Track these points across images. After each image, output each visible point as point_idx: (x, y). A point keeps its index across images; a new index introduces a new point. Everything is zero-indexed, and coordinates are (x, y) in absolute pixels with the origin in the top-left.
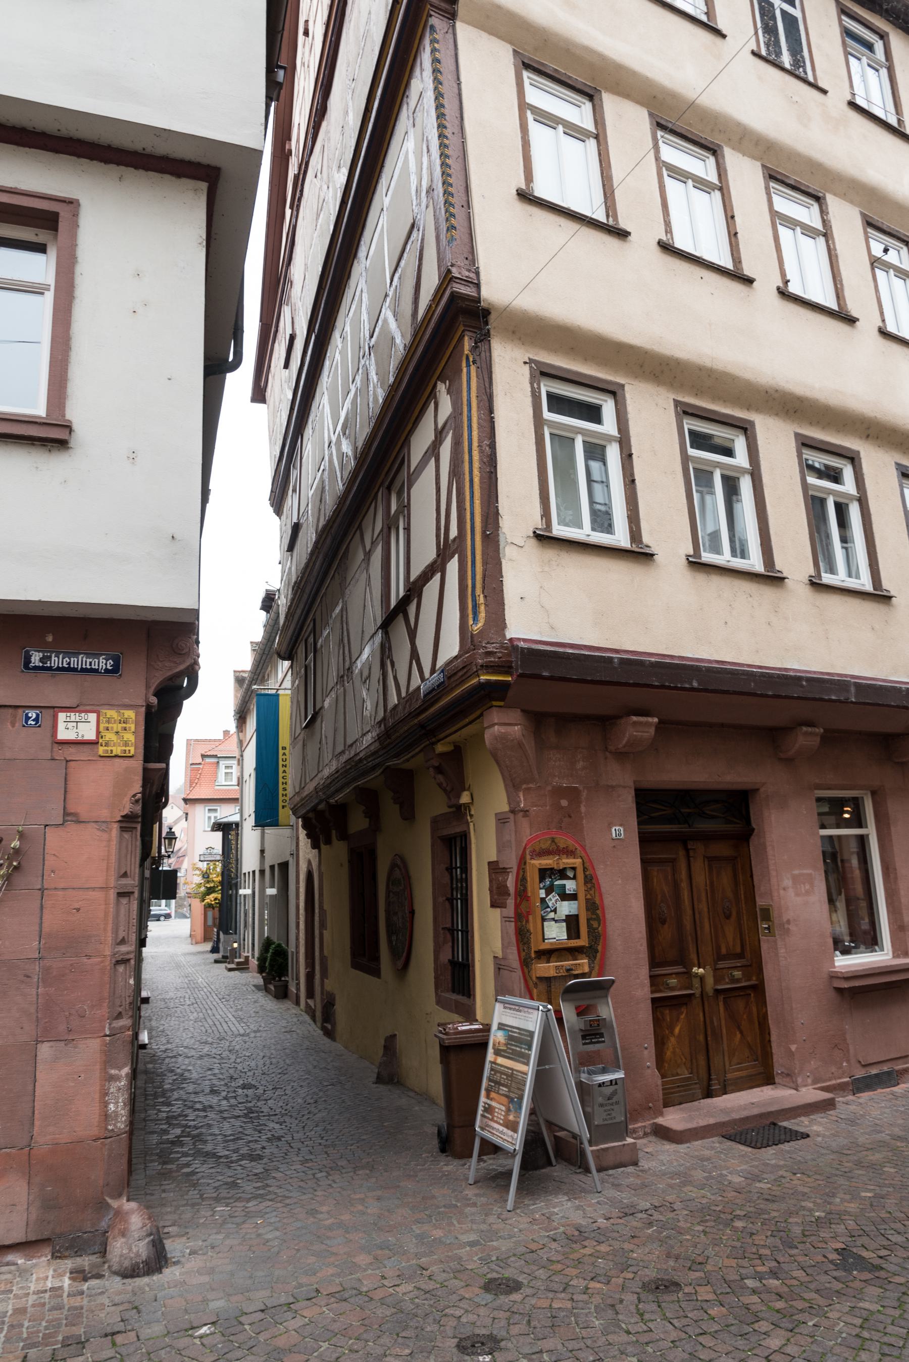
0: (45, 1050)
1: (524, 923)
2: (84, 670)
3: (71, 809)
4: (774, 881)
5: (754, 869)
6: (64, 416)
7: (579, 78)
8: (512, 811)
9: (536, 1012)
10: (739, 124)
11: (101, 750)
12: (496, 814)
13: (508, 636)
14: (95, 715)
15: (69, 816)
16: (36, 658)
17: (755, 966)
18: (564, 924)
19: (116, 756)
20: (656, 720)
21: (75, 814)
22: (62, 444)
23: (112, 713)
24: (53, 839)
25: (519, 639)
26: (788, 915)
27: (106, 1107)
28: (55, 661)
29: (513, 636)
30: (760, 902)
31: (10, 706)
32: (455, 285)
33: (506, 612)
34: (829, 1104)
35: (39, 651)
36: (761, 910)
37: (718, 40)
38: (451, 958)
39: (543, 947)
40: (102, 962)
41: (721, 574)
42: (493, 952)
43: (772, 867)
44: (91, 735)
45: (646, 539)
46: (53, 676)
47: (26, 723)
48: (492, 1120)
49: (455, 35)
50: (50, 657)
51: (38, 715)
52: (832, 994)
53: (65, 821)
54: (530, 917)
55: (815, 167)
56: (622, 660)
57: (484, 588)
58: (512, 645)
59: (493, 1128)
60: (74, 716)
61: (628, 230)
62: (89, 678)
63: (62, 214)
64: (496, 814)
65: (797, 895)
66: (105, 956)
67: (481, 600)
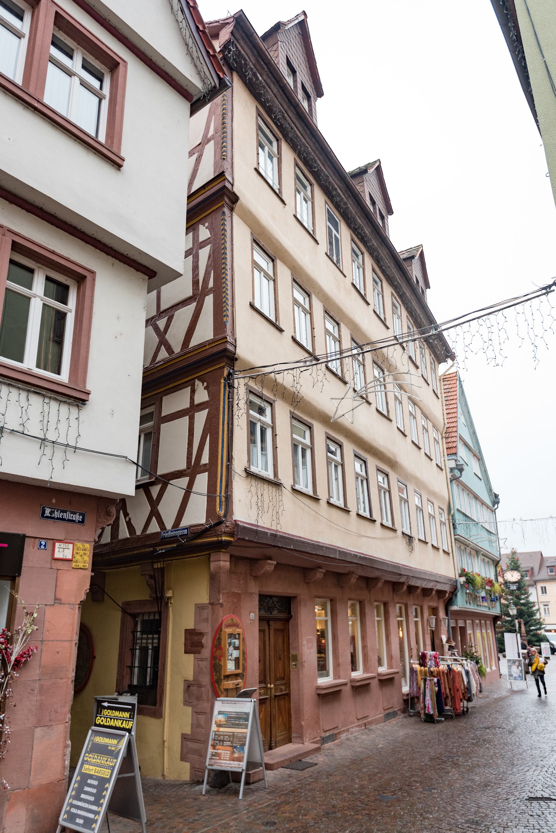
0: (38, 732)
1: (218, 661)
2: (69, 520)
3: (58, 596)
4: (300, 641)
5: (290, 635)
6: (85, 387)
7: (270, 252)
8: (211, 604)
9: (250, 703)
10: (320, 286)
11: (74, 565)
12: (196, 604)
13: (234, 519)
14: (72, 545)
15: (57, 601)
16: (47, 512)
17: (288, 685)
18: (234, 662)
19: (80, 568)
20: (275, 563)
21: (59, 599)
23: (79, 545)
24: (49, 612)
25: (241, 521)
26: (305, 658)
27: (64, 762)
28: (57, 514)
29: (237, 519)
30: (292, 652)
31: (33, 537)
32: (228, 345)
33: (234, 507)
34: (318, 750)
35: (49, 508)
36: (292, 655)
37: (316, 245)
38: (129, 683)
39: (227, 673)
40: (67, 681)
41: (301, 495)
42: (184, 678)
43: (300, 635)
44: (69, 557)
46: (54, 522)
47: (40, 547)
48: (220, 759)
49: (232, 219)
50: (54, 512)
51: (46, 543)
52: (316, 696)
53: (55, 603)
54: (222, 659)
55: (340, 311)
58: (236, 524)
59: (221, 763)
60: (63, 545)
61: (283, 329)
62: (70, 524)
63: (88, 278)
64: (196, 604)
65: (308, 648)
66: (69, 678)
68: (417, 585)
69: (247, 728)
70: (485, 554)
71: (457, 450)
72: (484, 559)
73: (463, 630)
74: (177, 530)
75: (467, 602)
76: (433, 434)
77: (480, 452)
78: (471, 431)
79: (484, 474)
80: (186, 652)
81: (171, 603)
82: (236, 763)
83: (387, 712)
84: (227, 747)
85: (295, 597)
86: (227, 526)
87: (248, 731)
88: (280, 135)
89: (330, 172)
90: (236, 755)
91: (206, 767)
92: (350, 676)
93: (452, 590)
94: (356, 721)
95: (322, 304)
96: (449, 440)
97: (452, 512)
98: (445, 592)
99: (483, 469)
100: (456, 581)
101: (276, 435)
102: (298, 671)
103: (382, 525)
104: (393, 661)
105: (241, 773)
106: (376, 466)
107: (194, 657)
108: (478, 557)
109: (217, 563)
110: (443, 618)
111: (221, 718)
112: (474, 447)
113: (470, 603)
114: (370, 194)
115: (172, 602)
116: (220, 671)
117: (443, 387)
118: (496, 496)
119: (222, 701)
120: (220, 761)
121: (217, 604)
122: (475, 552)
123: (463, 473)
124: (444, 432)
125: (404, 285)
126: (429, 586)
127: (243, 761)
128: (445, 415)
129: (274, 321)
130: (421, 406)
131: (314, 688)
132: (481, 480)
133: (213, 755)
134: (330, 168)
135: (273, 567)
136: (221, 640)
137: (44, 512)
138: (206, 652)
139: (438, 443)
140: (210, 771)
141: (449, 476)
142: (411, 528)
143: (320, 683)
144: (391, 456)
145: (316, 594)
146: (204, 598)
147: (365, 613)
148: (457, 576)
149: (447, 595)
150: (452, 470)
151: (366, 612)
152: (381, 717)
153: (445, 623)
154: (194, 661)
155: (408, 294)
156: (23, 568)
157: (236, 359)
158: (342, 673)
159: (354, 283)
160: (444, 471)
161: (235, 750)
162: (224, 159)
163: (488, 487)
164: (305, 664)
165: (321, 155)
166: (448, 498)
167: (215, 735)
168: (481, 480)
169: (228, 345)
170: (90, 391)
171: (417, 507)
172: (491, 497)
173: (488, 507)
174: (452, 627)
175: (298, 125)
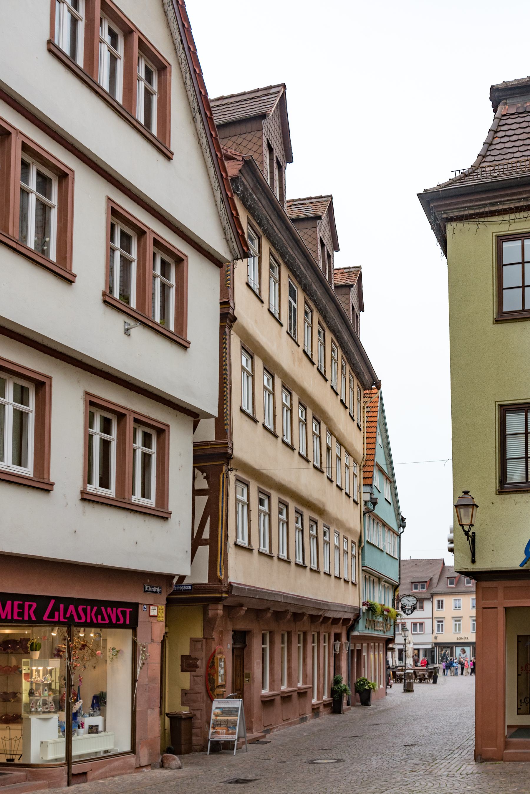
0: (149, 711)
4: (252, 664)
12: (191, 638)
22: (166, 519)
23: (160, 607)
28: (151, 589)
30: (246, 672)
36: (246, 674)
39: (219, 684)
43: (252, 659)
44: (156, 614)
45: (252, 544)
54: (215, 675)
56: (248, 589)
57: (224, 563)
58: (230, 585)
64: (191, 638)
67: (223, 568)
68: (330, 616)
69: (237, 715)
70: (386, 580)
71: (372, 481)
72: (384, 585)
73: (359, 652)
74: (181, 586)
75: (366, 628)
76: (354, 469)
77: (393, 474)
78: (387, 452)
79: (394, 497)
80: (182, 671)
81: (167, 637)
82: (230, 736)
83: (301, 717)
84: (223, 728)
85: (250, 631)
86: (225, 587)
87: (238, 718)
88: (260, 231)
89: (297, 253)
90: (230, 732)
91: (209, 739)
92: (280, 689)
93: (355, 618)
94: (282, 721)
95: (281, 380)
96: (366, 469)
97: (363, 544)
98: (350, 619)
99: (394, 492)
100: (360, 609)
101: (250, 511)
102: (250, 685)
103: (311, 569)
104: (308, 679)
105: (234, 741)
106: (309, 516)
107: (190, 674)
108: (379, 584)
109: (215, 611)
110: (345, 643)
111: (218, 711)
112: (388, 472)
113: (368, 628)
114: (321, 238)
115: (168, 635)
116: (214, 682)
117: (366, 415)
118: (403, 519)
119: (218, 701)
120: (219, 736)
121: (210, 639)
122: (378, 579)
123: (376, 507)
124: (362, 465)
125: (344, 330)
126: (339, 615)
127: (235, 735)
128: (365, 444)
129: (252, 415)
130: (346, 445)
131: (260, 697)
132: (390, 504)
133: (213, 733)
134: (297, 250)
135: (244, 612)
136: (215, 663)
137: (145, 589)
138: (202, 670)
139: (356, 476)
140: (211, 741)
141: (363, 509)
142: (330, 567)
143: (264, 693)
144: (320, 506)
145: (263, 628)
146: (199, 634)
147: (291, 641)
148: (361, 604)
149: (351, 622)
150: (366, 502)
151: (293, 641)
152: (297, 720)
153: (346, 647)
154: (190, 677)
155: (346, 338)
156: (139, 622)
157: (232, 458)
158: (276, 687)
159: (306, 350)
160: (359, 505)
161: (229, 729)
162: (228, 287)
163: (396, 511)
164: (256, 680)
165: (292, 242)
166: (359, 531)
167: (214, 721)
168: (390, 504)
169: (229, 450)
170: (171, 512)
171: (336, 546)
172: (398, 521)
173: (394, 532)
174: (351, 650)
175: (277, 223)
